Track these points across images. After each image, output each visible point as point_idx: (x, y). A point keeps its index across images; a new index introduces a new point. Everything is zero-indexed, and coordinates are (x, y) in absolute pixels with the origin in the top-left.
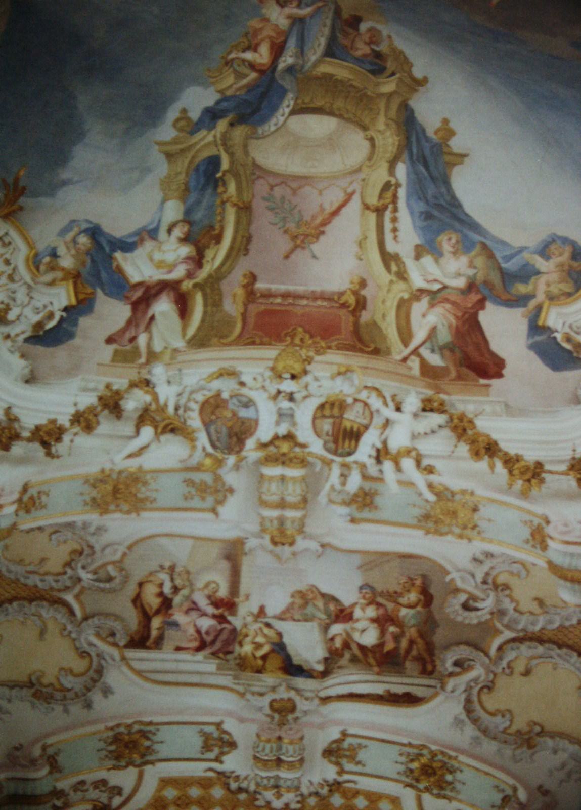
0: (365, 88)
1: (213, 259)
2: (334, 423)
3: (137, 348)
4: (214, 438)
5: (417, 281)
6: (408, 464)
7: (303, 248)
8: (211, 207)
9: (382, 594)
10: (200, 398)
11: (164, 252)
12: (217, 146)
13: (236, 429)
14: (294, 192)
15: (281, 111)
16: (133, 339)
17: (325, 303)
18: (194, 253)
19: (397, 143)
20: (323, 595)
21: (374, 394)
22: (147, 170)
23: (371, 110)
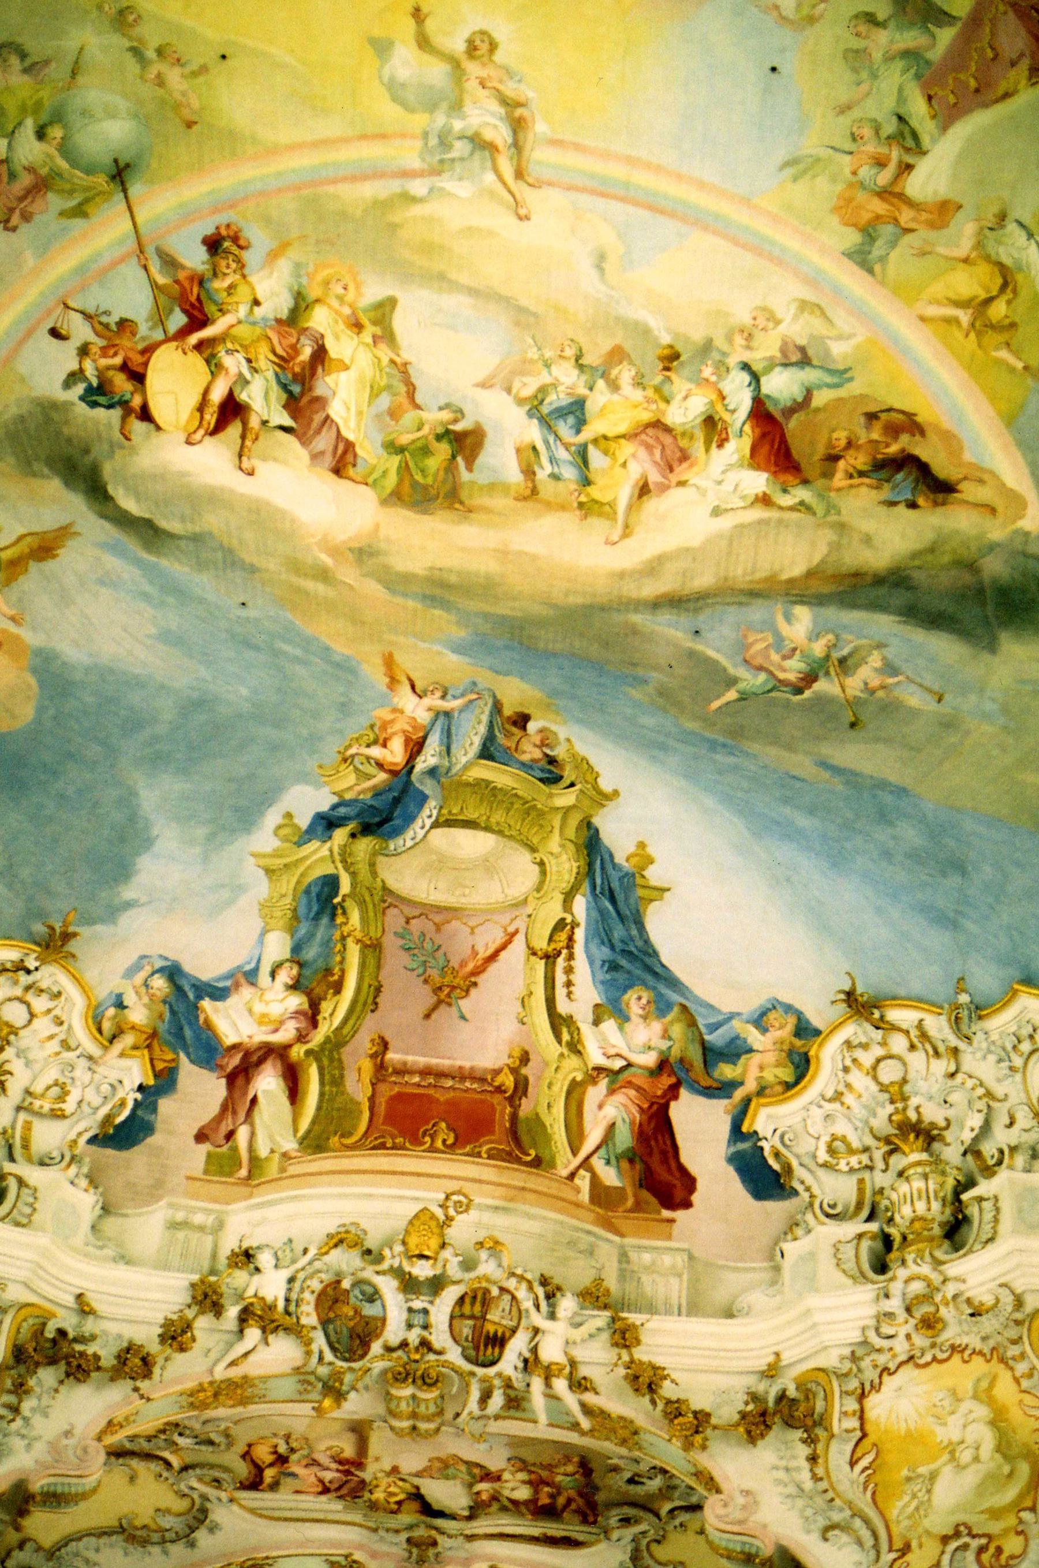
0: (534, 799)
1: (331, 1015)
2: (475, 1326)
3: (235, 1149)
4: (333, 1339)
5: (595, 1057)
6: (560, 1385)
7: (450, 1005)
8: (327, 943)
9: (534, 1464)
10: (316, 1285)
11: (267, 1003)
12: (333, 862)
13: (359, 1330)
14: (438, 928)
15: (419, 822)
16: (230, 1135)
17: (475, 1086)
18: (306, 1006)
19: (575, 870)
20: (466, 1463)
21: (524, 1286)
22: (239, 889)
23: (541, 826)
